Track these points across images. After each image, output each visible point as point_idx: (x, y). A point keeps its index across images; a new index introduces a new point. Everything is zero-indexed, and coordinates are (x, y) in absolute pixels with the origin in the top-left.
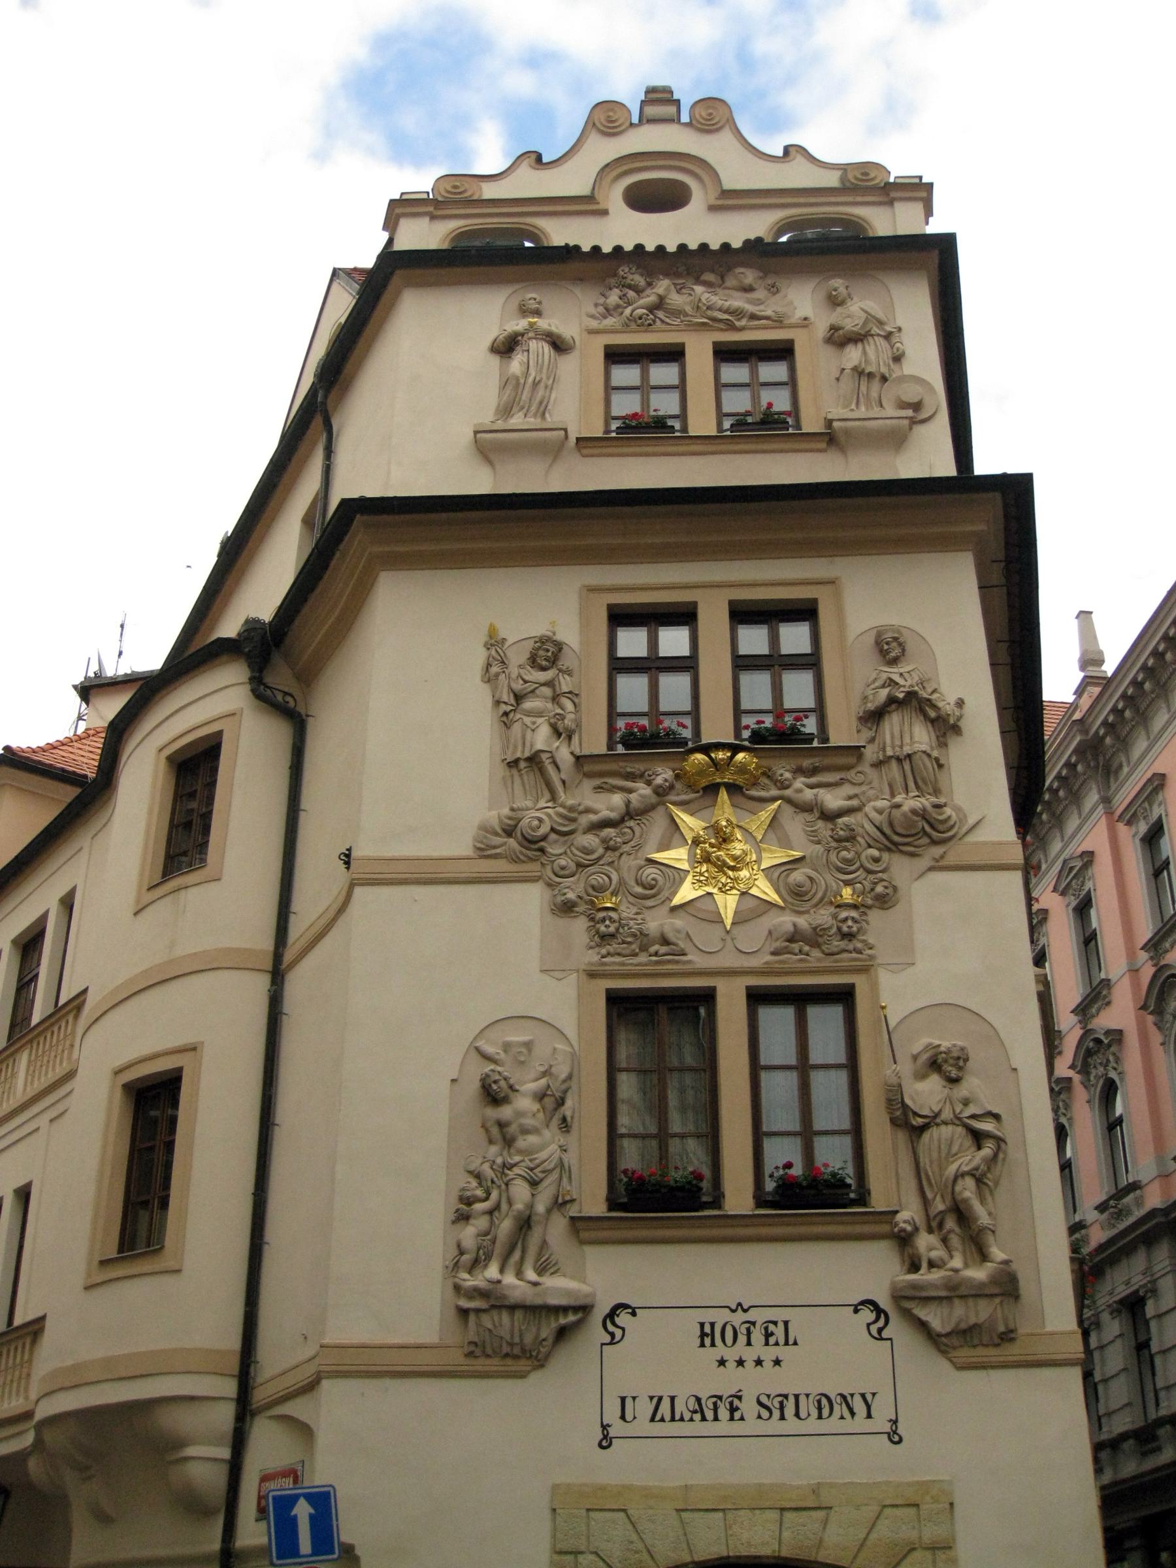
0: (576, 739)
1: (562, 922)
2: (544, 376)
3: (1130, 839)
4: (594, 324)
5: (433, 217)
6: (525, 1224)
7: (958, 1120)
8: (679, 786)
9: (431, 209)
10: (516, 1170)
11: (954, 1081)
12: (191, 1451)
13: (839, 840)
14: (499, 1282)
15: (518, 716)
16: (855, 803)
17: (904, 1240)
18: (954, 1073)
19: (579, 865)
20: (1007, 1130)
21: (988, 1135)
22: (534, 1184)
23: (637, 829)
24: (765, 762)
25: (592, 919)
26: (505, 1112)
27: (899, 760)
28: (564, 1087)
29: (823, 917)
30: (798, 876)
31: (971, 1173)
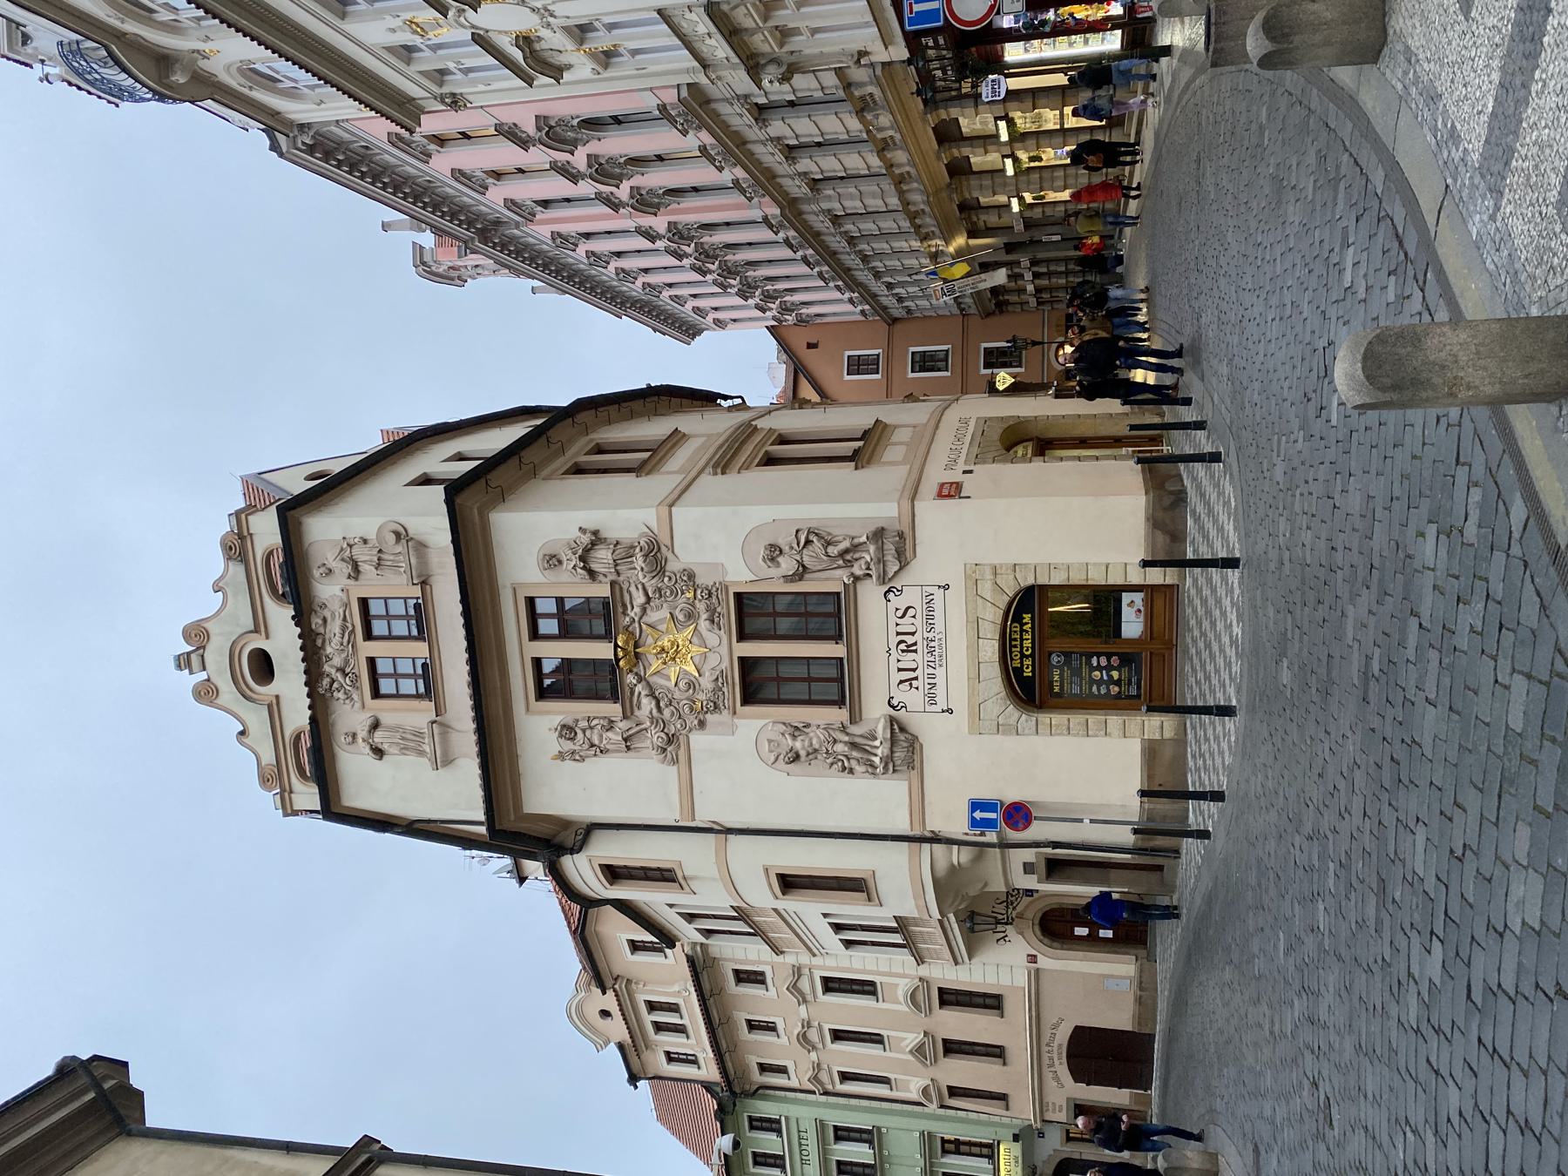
0: (613, 719)
1: (708, 726)
2: (398, 735)
3: (541, 214)
4: (358, 705)
5: (291, 792)
6: (854, 746)
7: (800, 552)
8: (635, 670)
9: (286, 794)
11: (781, 551)
12: (956, 863)
13: (661, 596)
16: (640, 586)
17: (857, 579)
18: (778, 553)
19: (680, 718)
20: (805, 526)
21: (807, 538)
22: (835, 741)
24: (621, 629)
25: (707, 712)
26: (803, 753)
27: (616, 565)
29: (701, 606)
30: (681, 617)
31: (826, 548)
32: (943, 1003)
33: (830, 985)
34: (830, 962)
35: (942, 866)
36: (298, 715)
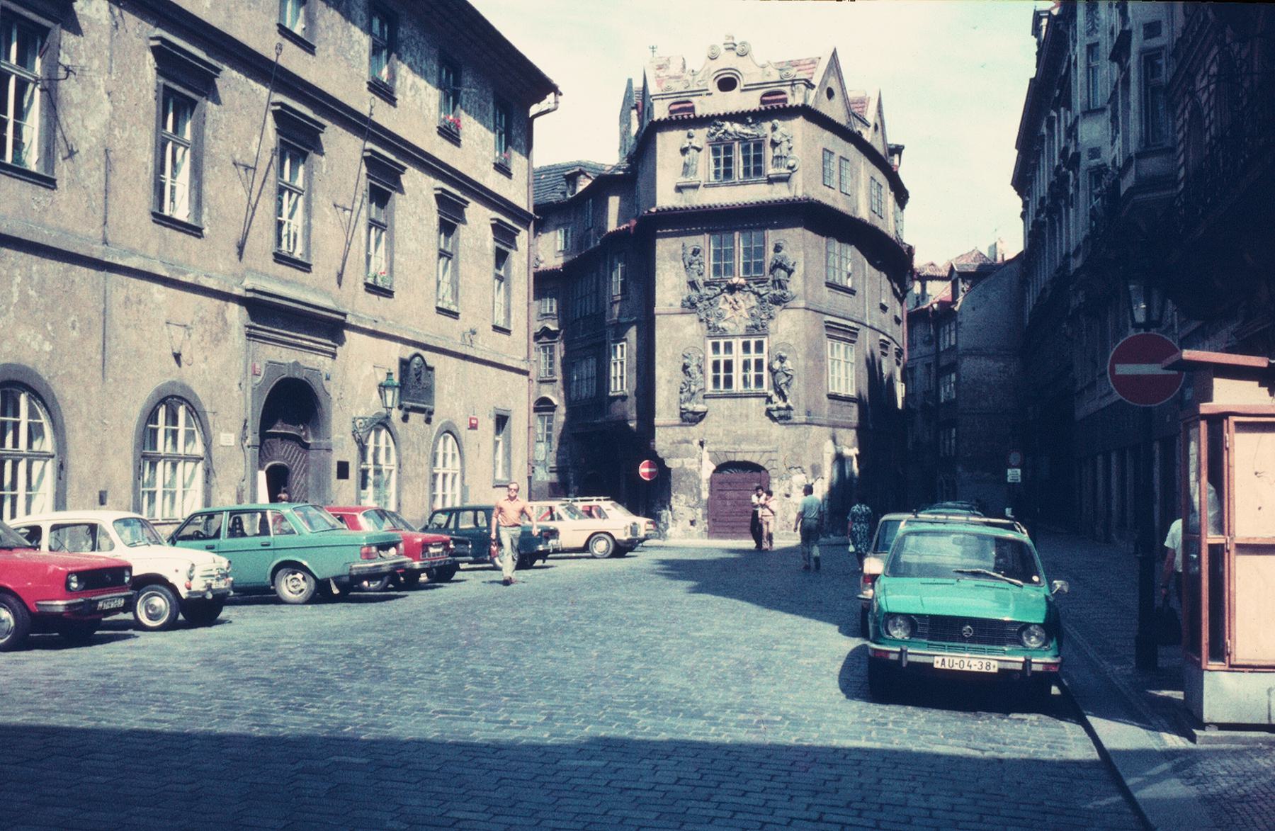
11: (782, 362)
36: (703, 107)
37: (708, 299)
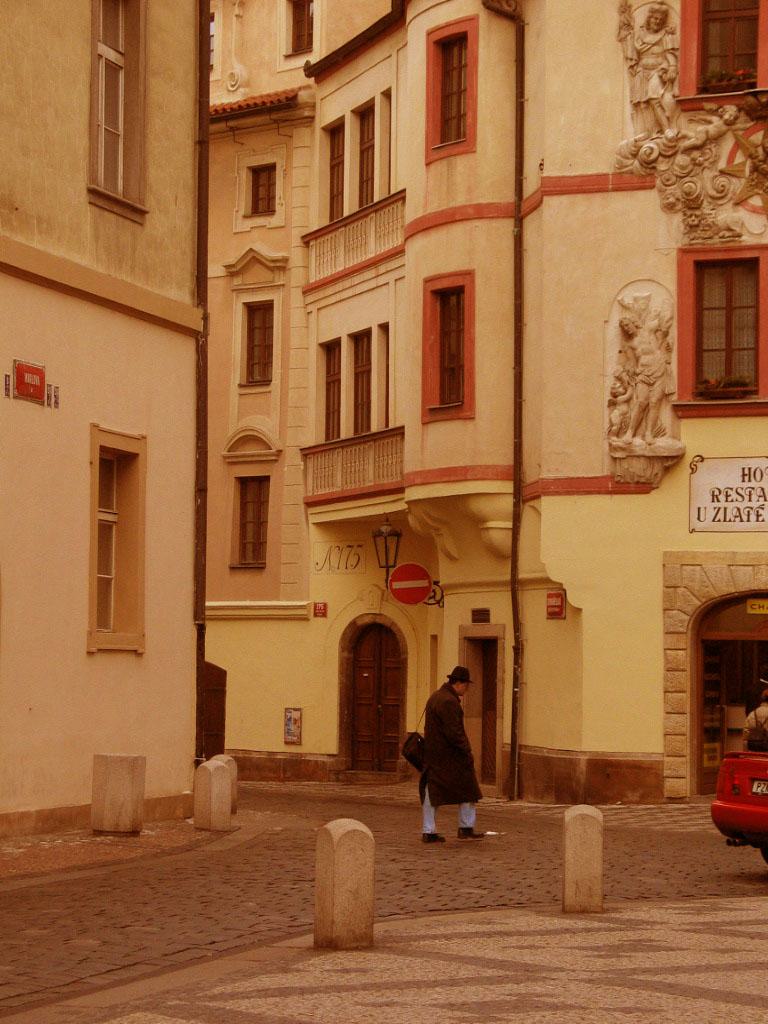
10: (640, 377)
12: (491, 524)
14: (630, 443)
15: (640, 69)
19: (677, 176)
22: (650, 385)
23: (713, 149)
25: (685, 215)
28: (669, 324)
32: (243, 482)
33: (259, 316)
34: (297, 317)
35: (481, 507)
37: (688, 150)
